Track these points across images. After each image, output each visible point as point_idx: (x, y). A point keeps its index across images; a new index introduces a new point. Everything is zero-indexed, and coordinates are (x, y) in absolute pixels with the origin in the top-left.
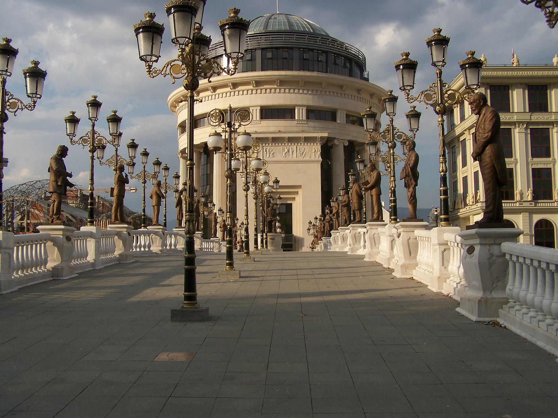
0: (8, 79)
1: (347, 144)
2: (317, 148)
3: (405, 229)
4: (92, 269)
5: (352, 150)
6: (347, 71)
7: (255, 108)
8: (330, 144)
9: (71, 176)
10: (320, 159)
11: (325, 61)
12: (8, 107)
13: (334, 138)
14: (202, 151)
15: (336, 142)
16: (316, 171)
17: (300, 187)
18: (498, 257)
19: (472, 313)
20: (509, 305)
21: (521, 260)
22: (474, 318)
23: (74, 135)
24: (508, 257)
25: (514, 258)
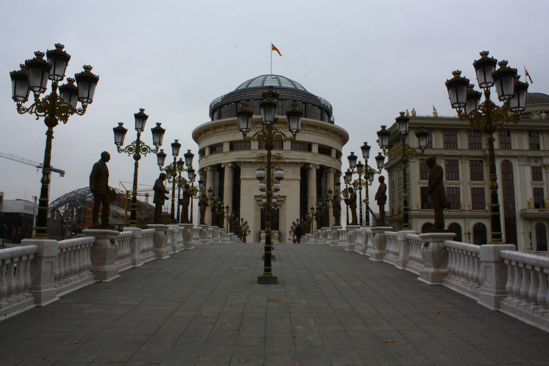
0: (142, 133)
1: (318, 168)
2: (298, 170)
3: (378, 231)
4: (173, 252)
5: (322, 171)
6: (319, 116)
8: (306, 168)
9: (168, 193)
10: (300, 178)
11: (304, 108)
13: (310, 164)
14: (216, 169)
15: (311, 166)
16: (297, 186)
17: (285, 197)
18: (443, 249)
19: (428, 280)
20: (449, 276)
21: (456, 251)
22: (429, 283)
23: (163, 165)
24: (448, 249)
25: (452, 250)
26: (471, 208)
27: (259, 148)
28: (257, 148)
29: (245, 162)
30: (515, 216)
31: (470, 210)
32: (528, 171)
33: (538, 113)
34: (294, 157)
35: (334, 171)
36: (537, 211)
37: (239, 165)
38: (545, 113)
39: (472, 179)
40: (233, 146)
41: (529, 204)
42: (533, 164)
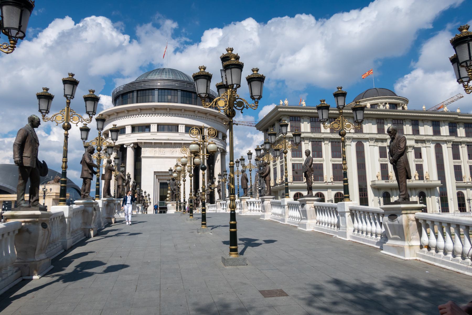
7: (154, 125)
12: (236, 106)
26: (332, 180)
27: (158, 131)
28: (156, 131)
29: (145, 143)
30: (366, 186)
31: (332, 182)
32: (377, 150)
33: (383, 104)
34: (188, 139)
35: (220, 150)
36: (383, 182)
37: (140, 145)
38: (389, 104)
39: (333, 156)
40: (135, 128)
41: (377, 177)
42: (380, 144)
